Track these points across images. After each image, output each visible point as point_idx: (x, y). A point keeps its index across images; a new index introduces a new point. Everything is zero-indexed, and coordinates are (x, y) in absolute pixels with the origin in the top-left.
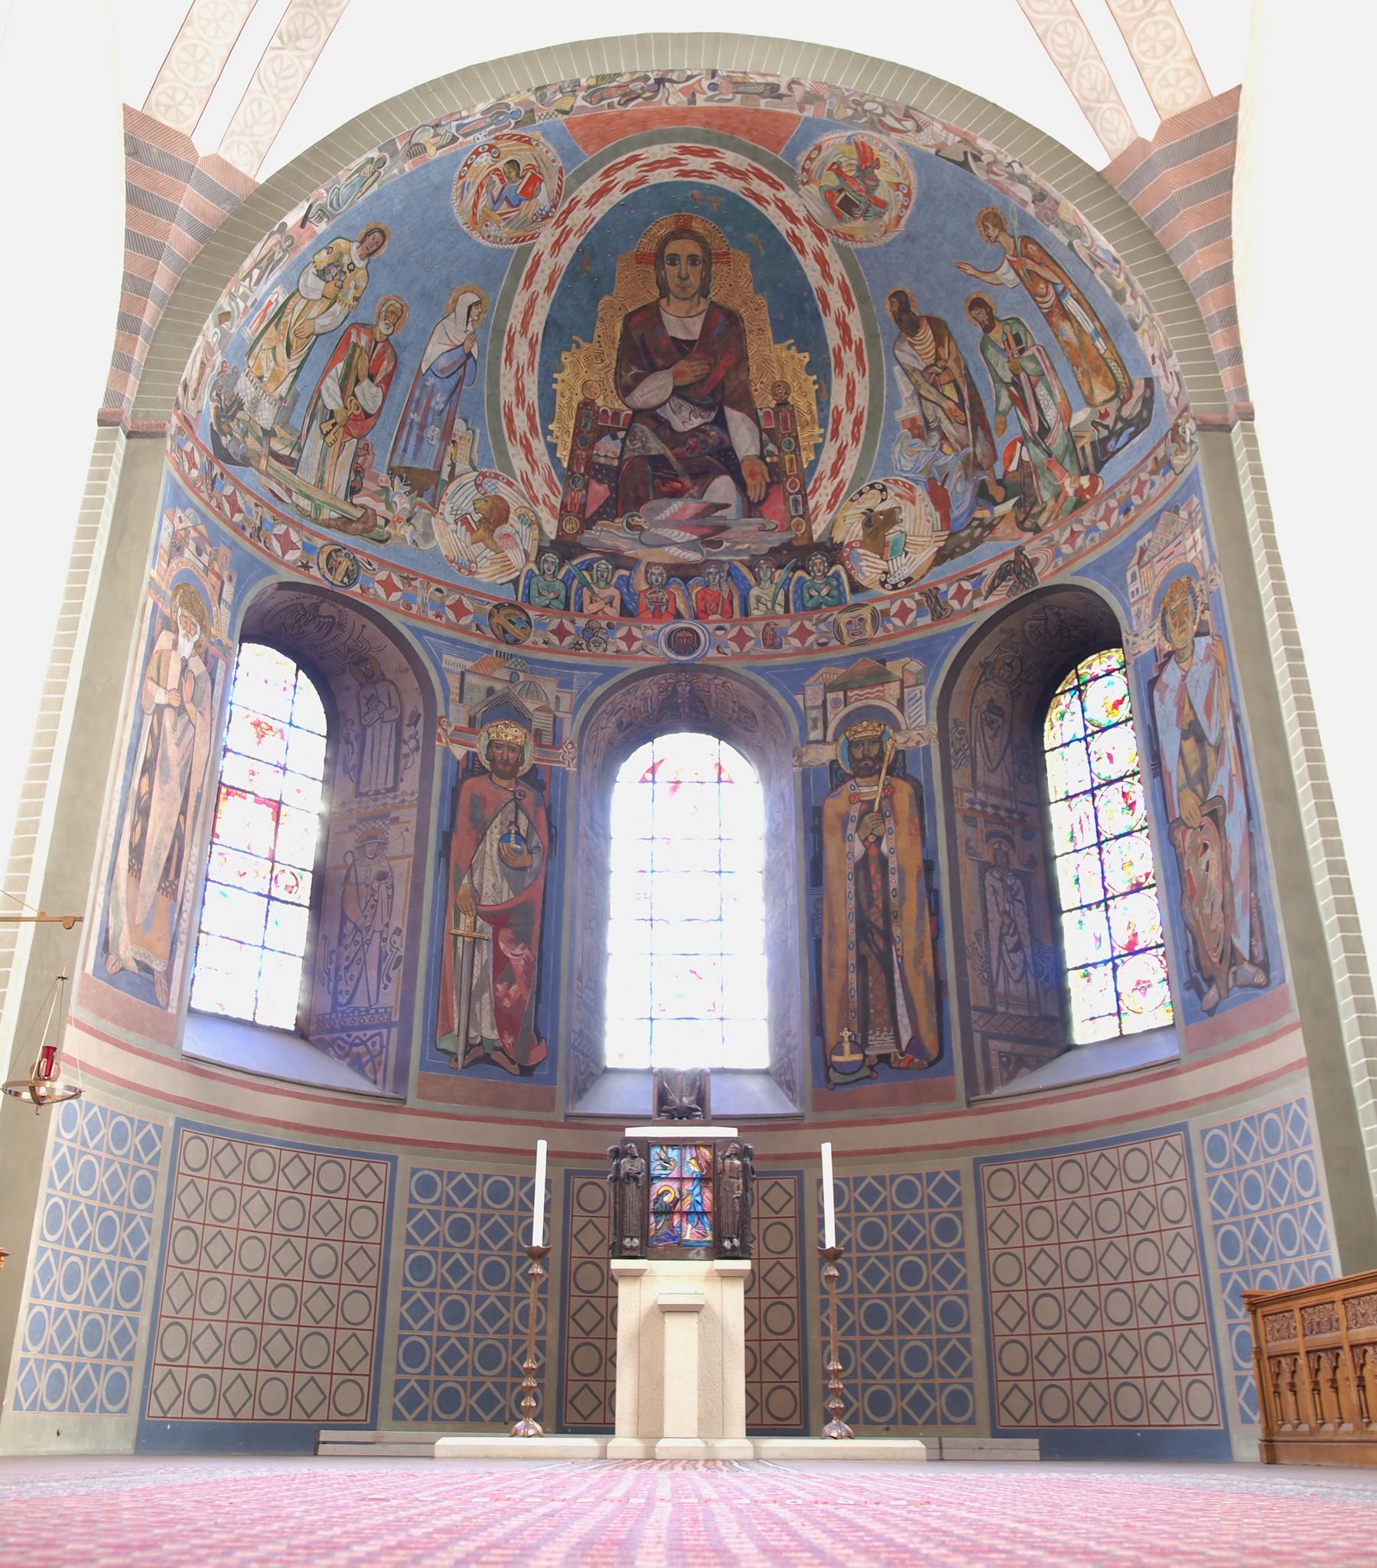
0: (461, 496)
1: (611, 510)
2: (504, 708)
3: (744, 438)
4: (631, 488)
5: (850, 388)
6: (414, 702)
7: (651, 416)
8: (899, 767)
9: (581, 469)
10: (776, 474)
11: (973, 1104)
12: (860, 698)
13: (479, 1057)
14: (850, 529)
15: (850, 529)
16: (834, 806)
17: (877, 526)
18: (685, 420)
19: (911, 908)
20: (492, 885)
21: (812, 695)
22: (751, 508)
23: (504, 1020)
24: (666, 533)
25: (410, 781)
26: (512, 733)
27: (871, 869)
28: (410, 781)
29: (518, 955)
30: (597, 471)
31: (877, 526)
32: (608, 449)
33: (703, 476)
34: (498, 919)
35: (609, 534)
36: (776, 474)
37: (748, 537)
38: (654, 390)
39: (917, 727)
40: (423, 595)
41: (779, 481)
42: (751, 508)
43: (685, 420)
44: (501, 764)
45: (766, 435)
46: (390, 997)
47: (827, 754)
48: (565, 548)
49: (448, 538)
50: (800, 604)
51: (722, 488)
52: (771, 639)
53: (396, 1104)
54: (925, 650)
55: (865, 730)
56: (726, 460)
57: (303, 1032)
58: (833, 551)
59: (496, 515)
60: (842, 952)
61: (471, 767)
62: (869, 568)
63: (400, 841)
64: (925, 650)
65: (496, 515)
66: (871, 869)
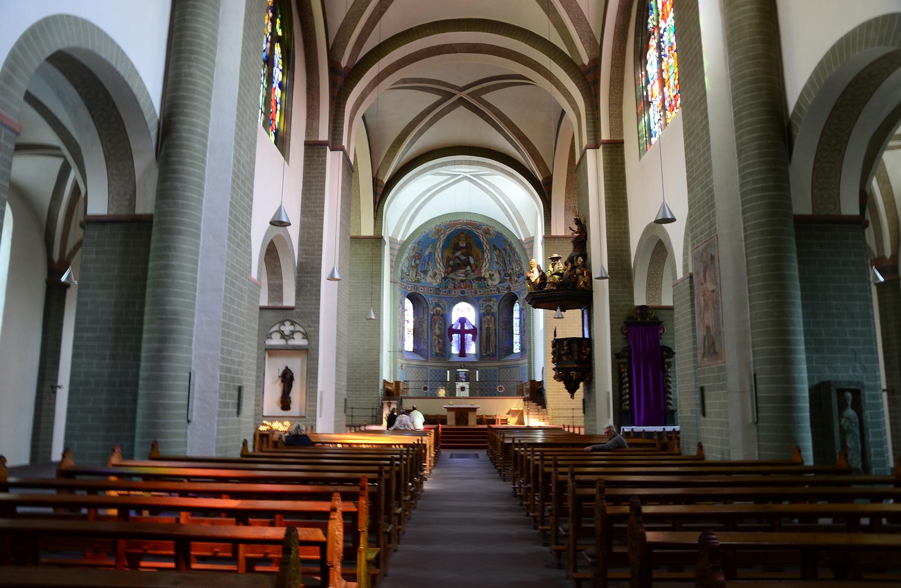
0: (430, 273)
1: (452, 272)
2: (438, 305)
3: (472, 261)
4: (455, 268)
5: (487, 255)
6: (425, 305)
7: (458, 257)
8: (493, 314)
9: (447, 266)
10: (477, 266)
11: (499, 361)
12: (488, 303)
13: (437, 355)
14: (487, 276)
15: (487, 276)
16: (484, 319)
17: (491, 276)
18: (463, 258)
19: (493, 335)
20: (437, 331)
21: (481, 302)
22: (473, 271)
23: (440, 350)
24: (460, 275)
25: (426, 317)
26: (439, 309)
27: (488, 329)
28: (426, 317)
29: (441, 341)
30: (450, 266)
31: (491, 276)
32: (451, 263)
33: (466, 266)
34: (438, 336)
35: (452, 275)
36: (477, 266)
37: (472, 276)
38: (458, 254)
39: (495, 309)
40: (426, 289)
41: (477, 268)
42: (473, 271)
43: (463, 258)
44: (438, 314)
45: (475, 260)
46: (425, 347)
47: (483, 311)
48: (445, 278)
49: (429, 279)
50: (480, 287)
51: (468, 268)
52: (476, 293)
53: (427, 361)
54: (497, 297)
55: (488, 308)
56: (469, 264)
57: (414, 351)
58: (485, 279)
59: (435, 274)
60: (484, 340)
61: (434, 315)
62: (490, 282)
63: (425, 326)
64: (497, 297)
65: (435, 274)
66: (488, 329)
